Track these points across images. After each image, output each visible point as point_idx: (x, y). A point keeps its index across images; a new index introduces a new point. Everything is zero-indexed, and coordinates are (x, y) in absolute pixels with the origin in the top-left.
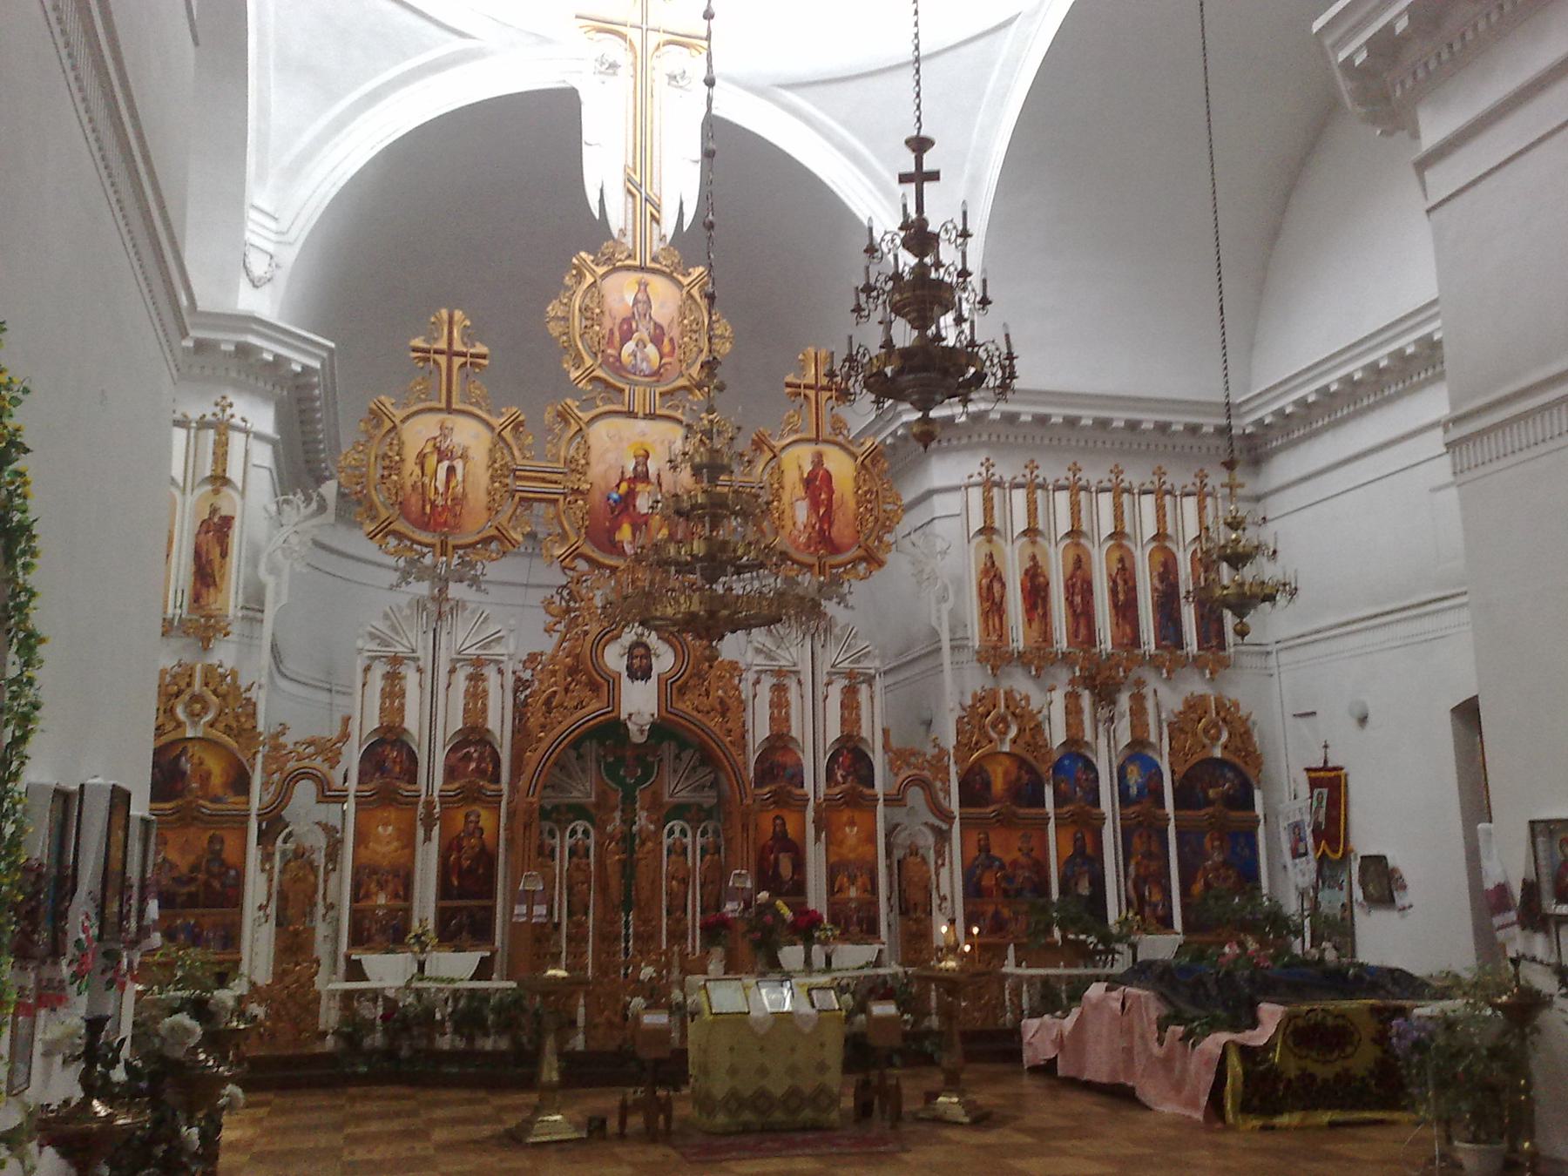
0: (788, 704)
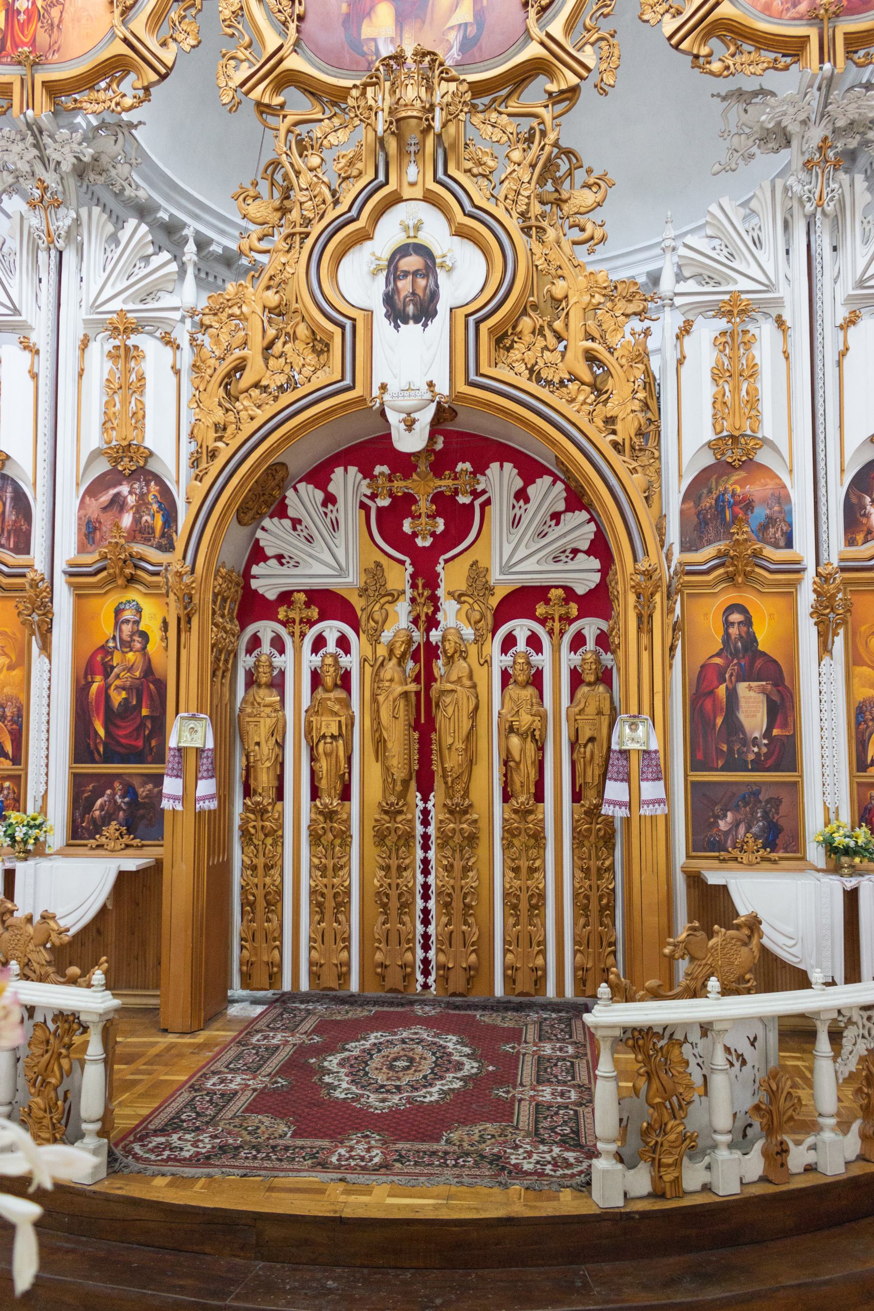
0: (753, 373)
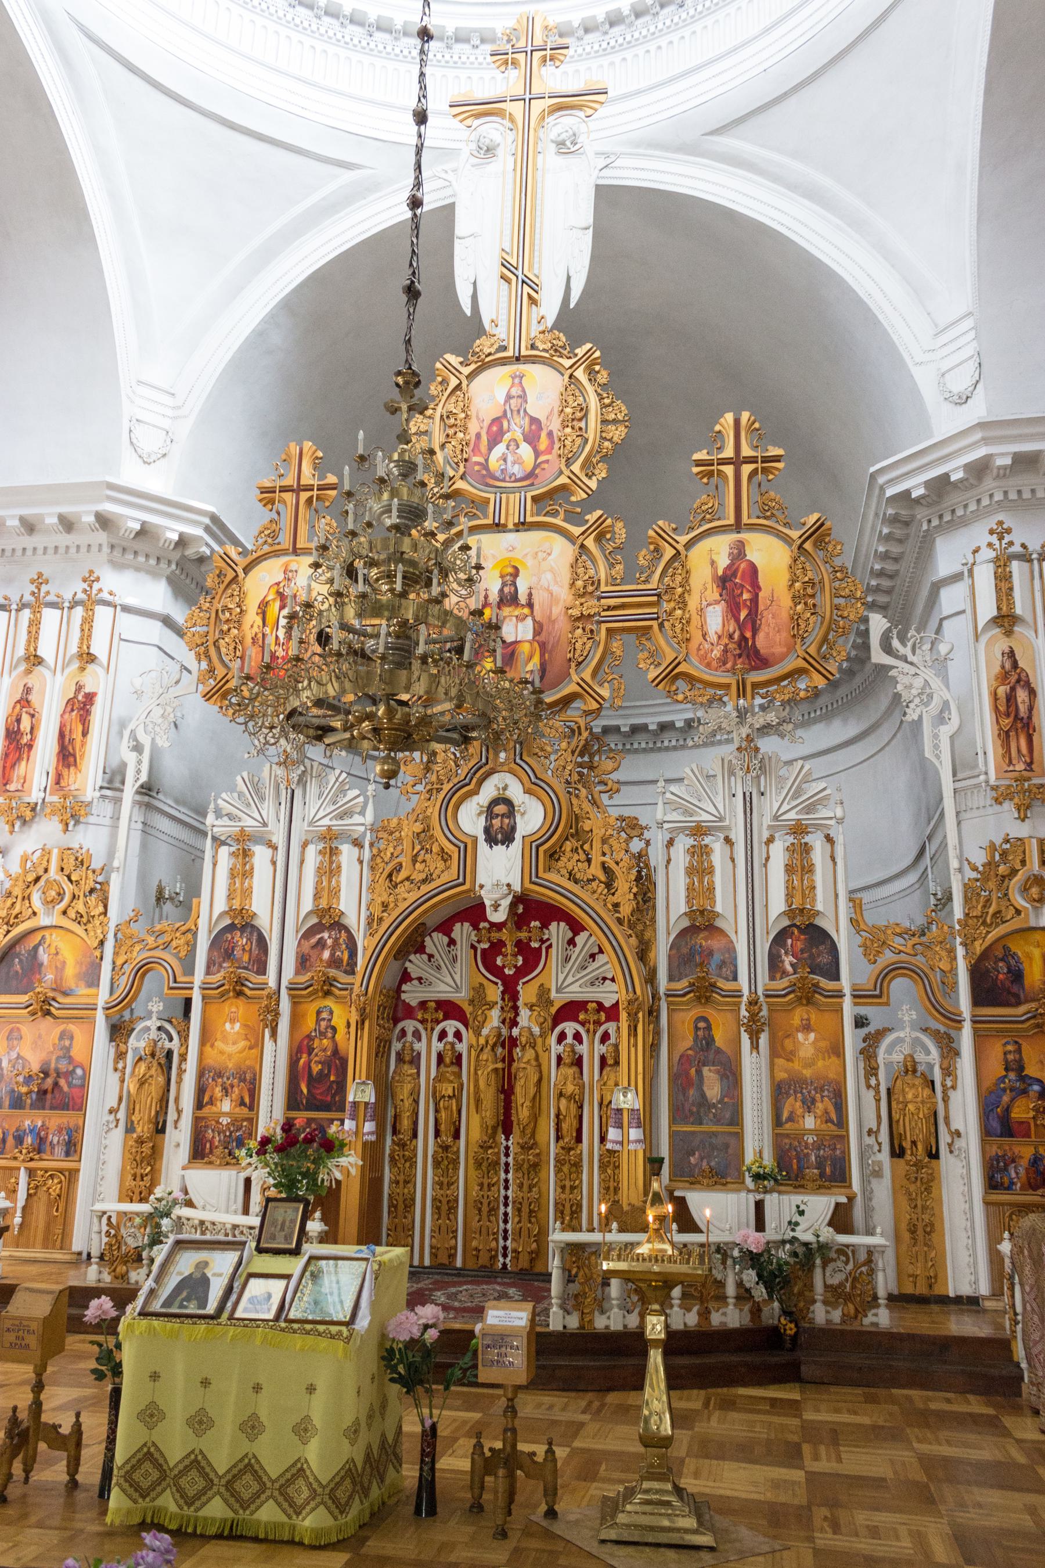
0: (711, 871)
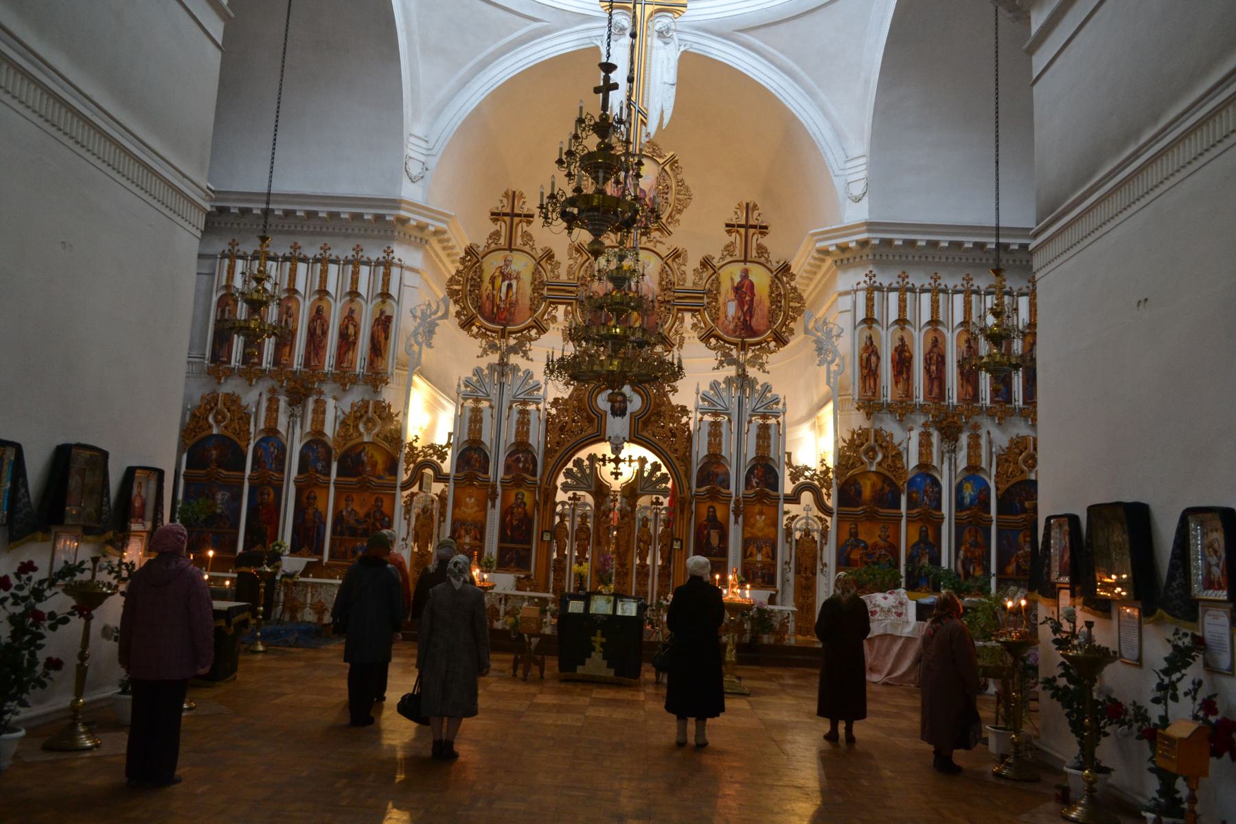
0: (721, 435)
